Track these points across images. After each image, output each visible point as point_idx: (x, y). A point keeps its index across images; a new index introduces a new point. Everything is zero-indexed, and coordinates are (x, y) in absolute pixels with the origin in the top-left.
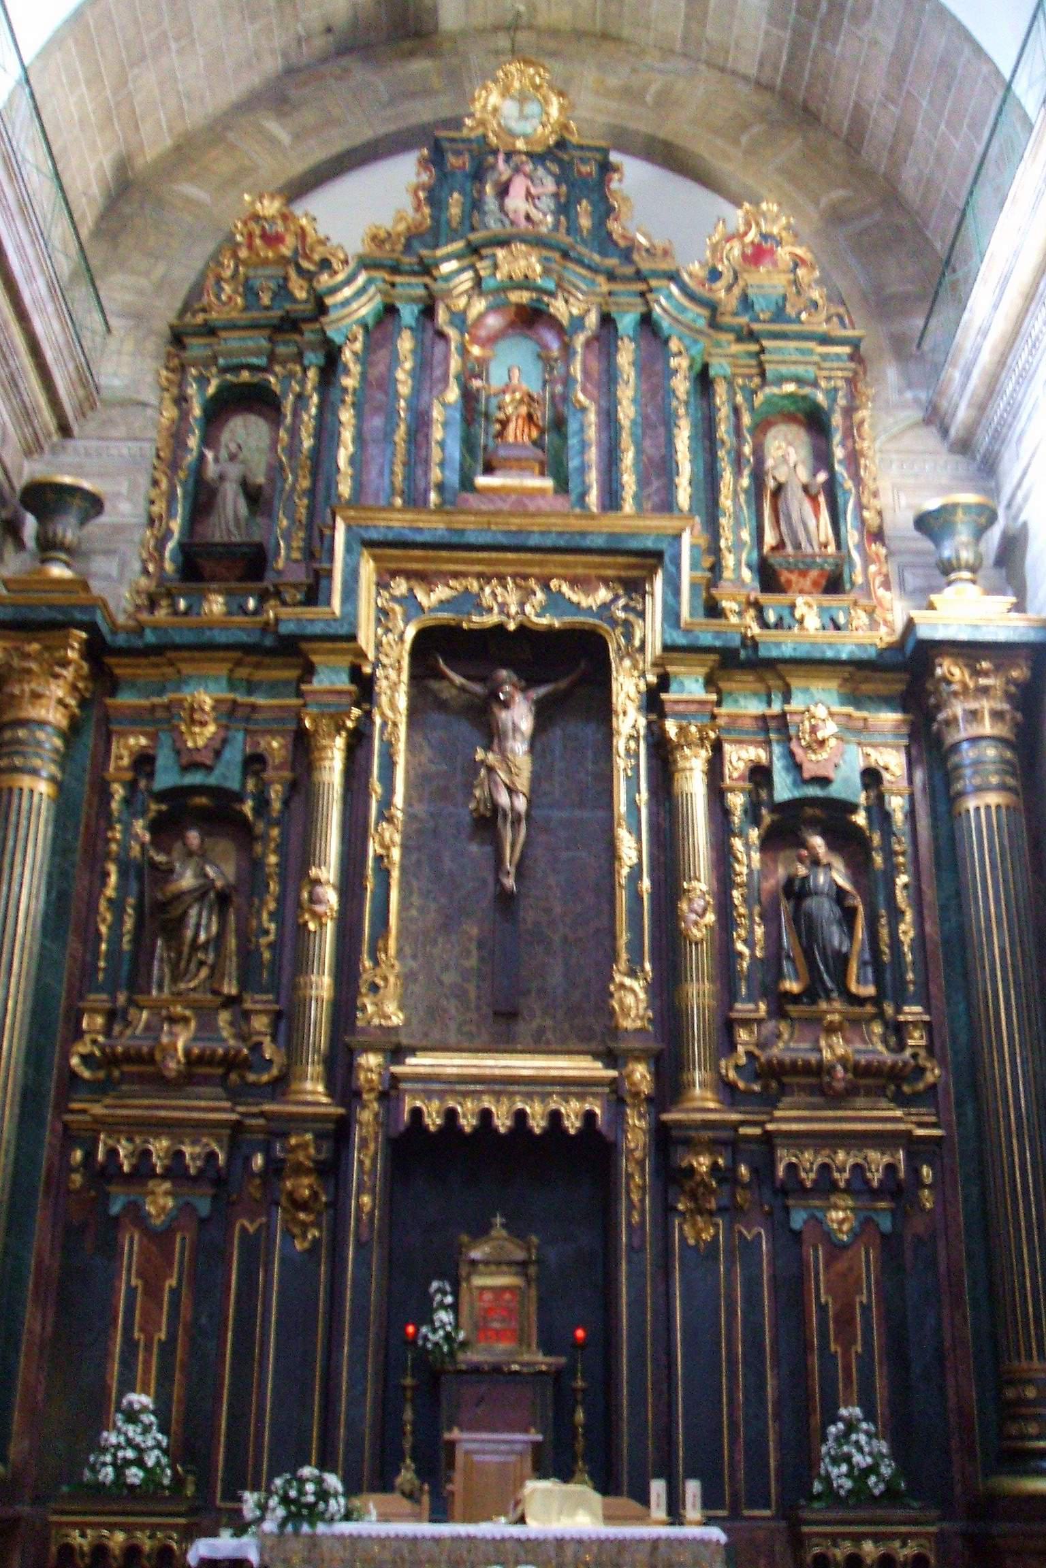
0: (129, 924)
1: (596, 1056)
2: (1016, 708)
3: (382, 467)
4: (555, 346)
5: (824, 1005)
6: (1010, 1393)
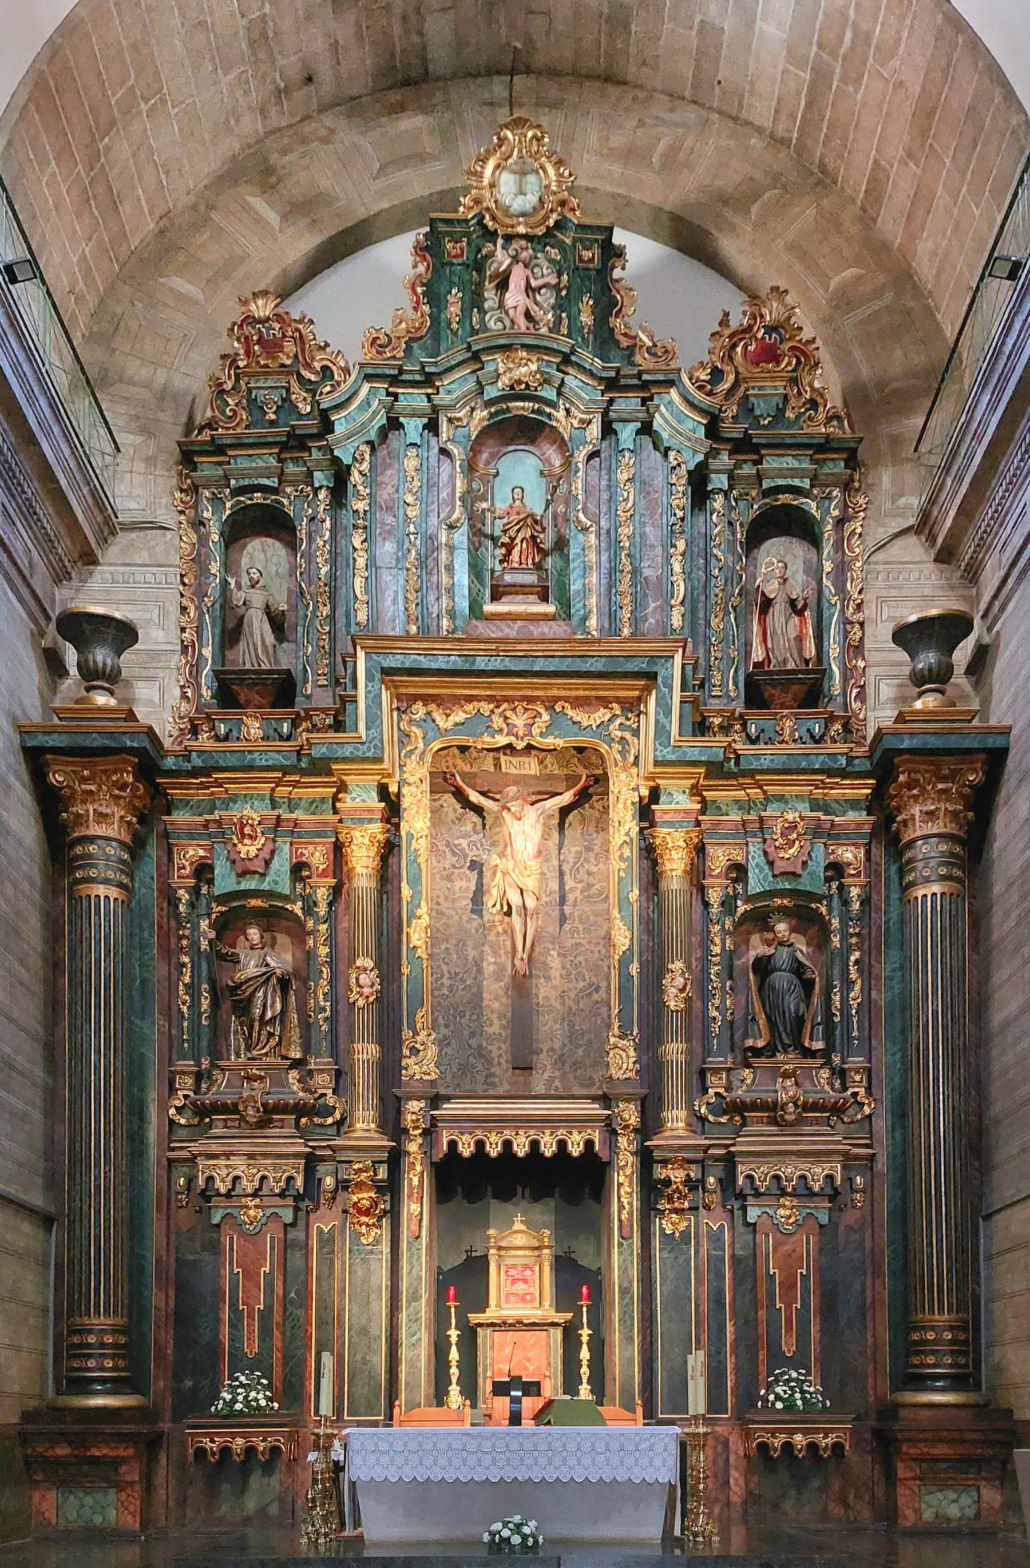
0: (205, 1004)
1: (594, 1099)
2: (968, 808)
3: (396, 592)
4: (557, 462)
5: (780, 1057)
6: (915, 1336)
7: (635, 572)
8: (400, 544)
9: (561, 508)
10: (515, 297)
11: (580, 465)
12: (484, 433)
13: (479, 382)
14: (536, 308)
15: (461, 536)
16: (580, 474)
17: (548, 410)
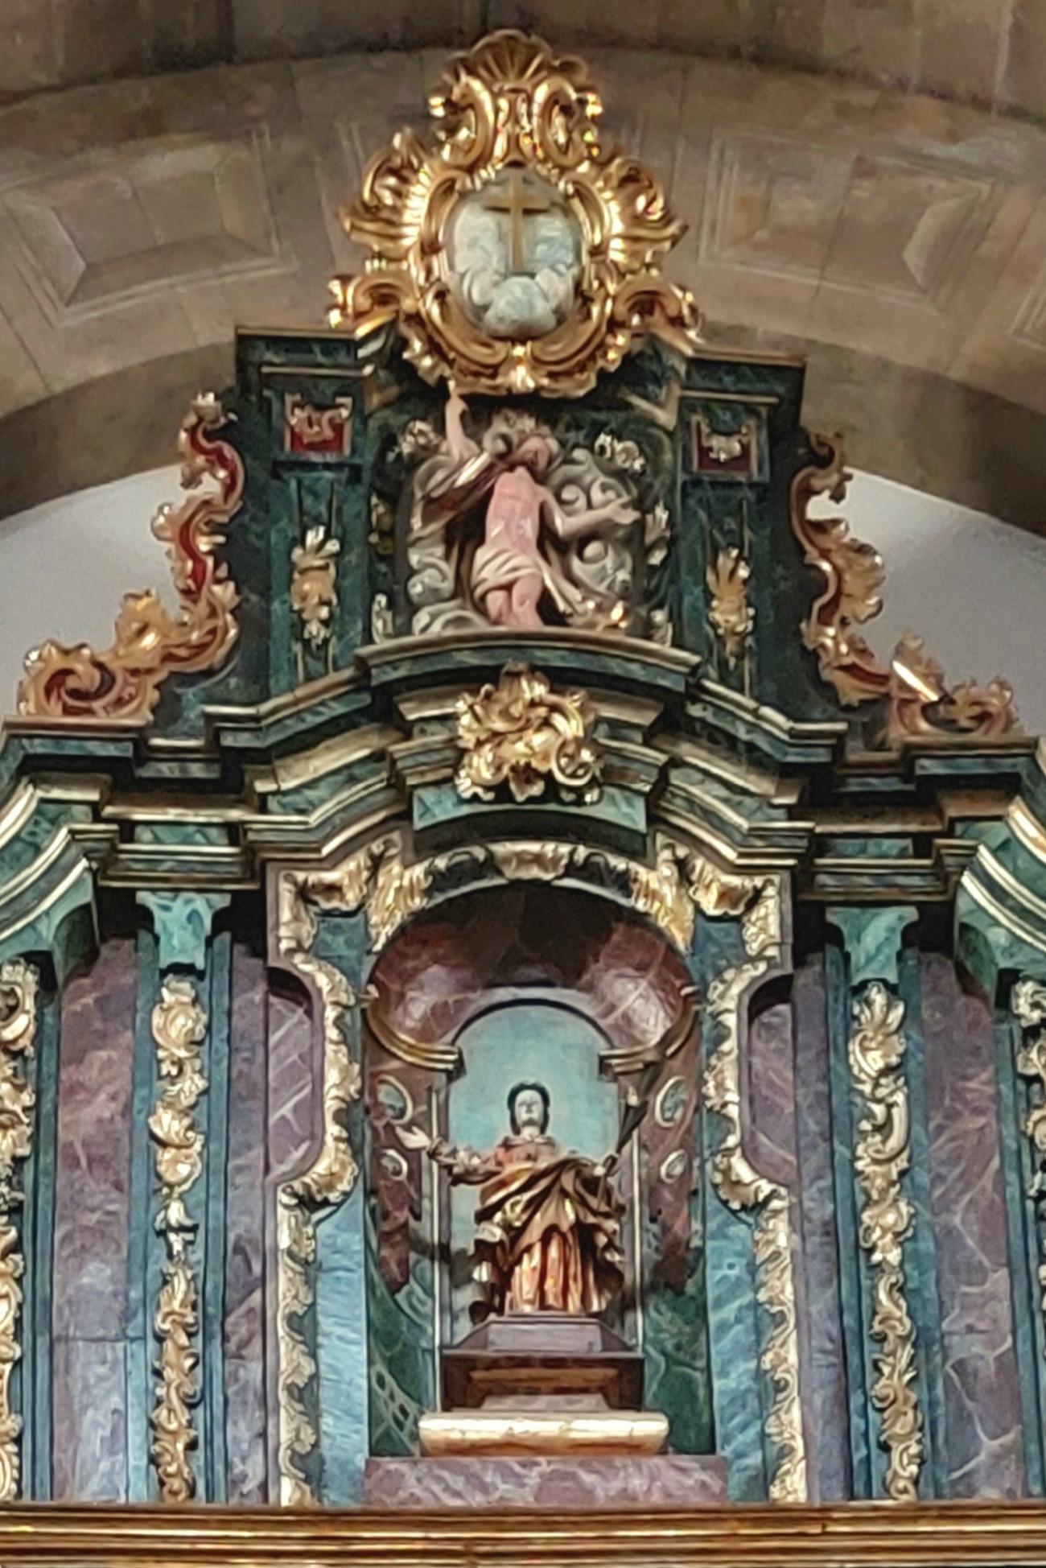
3: (121, 1415)
4: (654, 1023)
7: (923, 1340)
8: (135, 1265)
9: (672, 1164)
10: (505, 556)
11: (730, 1020)
12: (416, 932)
13: (396, 782)
14: (575, 594)
15: (344, 1237)
16: (729, 1045)
17: (619, 863)
